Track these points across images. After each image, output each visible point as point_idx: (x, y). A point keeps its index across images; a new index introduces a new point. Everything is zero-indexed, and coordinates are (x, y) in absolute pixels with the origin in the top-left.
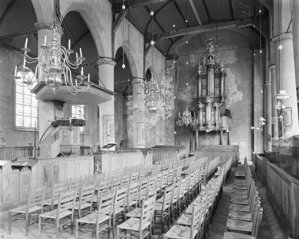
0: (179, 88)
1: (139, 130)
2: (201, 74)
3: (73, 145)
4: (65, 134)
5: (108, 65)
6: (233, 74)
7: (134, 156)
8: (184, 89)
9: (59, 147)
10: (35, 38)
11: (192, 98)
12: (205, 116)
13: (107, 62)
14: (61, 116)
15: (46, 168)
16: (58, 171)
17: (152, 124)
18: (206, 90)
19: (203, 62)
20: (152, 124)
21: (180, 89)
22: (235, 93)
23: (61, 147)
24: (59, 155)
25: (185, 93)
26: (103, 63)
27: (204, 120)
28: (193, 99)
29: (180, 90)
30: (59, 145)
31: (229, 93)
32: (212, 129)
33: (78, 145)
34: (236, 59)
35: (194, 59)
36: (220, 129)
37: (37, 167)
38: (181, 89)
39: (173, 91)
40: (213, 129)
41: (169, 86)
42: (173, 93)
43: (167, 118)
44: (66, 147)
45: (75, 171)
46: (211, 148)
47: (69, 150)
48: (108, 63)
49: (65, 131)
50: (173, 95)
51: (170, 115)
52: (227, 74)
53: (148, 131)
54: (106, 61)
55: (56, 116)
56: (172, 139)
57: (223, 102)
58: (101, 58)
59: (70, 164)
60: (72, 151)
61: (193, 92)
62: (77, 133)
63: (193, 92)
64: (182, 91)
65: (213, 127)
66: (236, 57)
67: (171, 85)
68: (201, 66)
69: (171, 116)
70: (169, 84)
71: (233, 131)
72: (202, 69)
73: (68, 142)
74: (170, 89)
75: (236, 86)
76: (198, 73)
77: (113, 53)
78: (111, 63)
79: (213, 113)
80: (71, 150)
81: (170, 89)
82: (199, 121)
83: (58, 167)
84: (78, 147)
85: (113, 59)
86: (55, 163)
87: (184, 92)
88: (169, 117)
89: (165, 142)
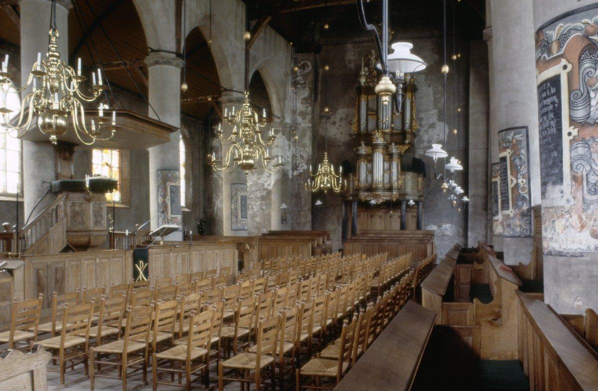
1: (235, 199)
2: (367, 85)
3: (94, 229)
4: (77, 208)
5: (167, 66)
6: (429, 86)
7: (217, 251)
8: (332, 115)
9: (65, 233)
10: (14, 13)
11: (349, 132)
12: (371, 172)
13: (165, 60)
14: (69, 171)
15: (41, 272)
16: (63, 278)
17: (266, 186)
18: (375, 117)
19: (370, 60)
20: (266, 186)
22: (432, 126)
23: (69, 233)
24: (66, 249)
25: (334, 123)
26: (157, 63)
27: (369, 179)
28: (351, 135)
30: (65, 229)
31: (421, 125)
33: (104, 231)
35: (352, 53)
37: (23, 271)
39: (309, 117)
40: (388, 198)
41: (300, 107)
42: (310, 123)
43: (295, 173)
44: (80, 234)
45: (96, 279)
46: (380, 235)
47: (85, 240)
48: (168, 63)
49: (78, 201)
50: (308, 127)
51: (303, 168)
52: (418, 87)
53: (257, 201)
54: (163, 58)
55: (59, 172)
56: (306, 218)
57: (409, 143)
58: (153, 51)
59: (85, 265)
60: (91, 241)
61: (351, 120)
62: (102, 206)
63: (351, 120)
67: (305, 106)
68: (366, 69)
69: (304, 170)
70: (301, 103)
71: (429, 203)
72: (367, 74)
73: (83, 223)
74: (303, 114)
75: (434, 112)
76: (360, 83)
77: (178, 41)
78: (175, 63)
79: (387, 165)
80: (90, 240)
81: (303, 114)
82: (359, 180)
83: (63, 271)
84: (104, 233)
85: (178, 55)
86: (58, 263)
87: (332, 120)
88: (301, 171)
89: (292, 224)
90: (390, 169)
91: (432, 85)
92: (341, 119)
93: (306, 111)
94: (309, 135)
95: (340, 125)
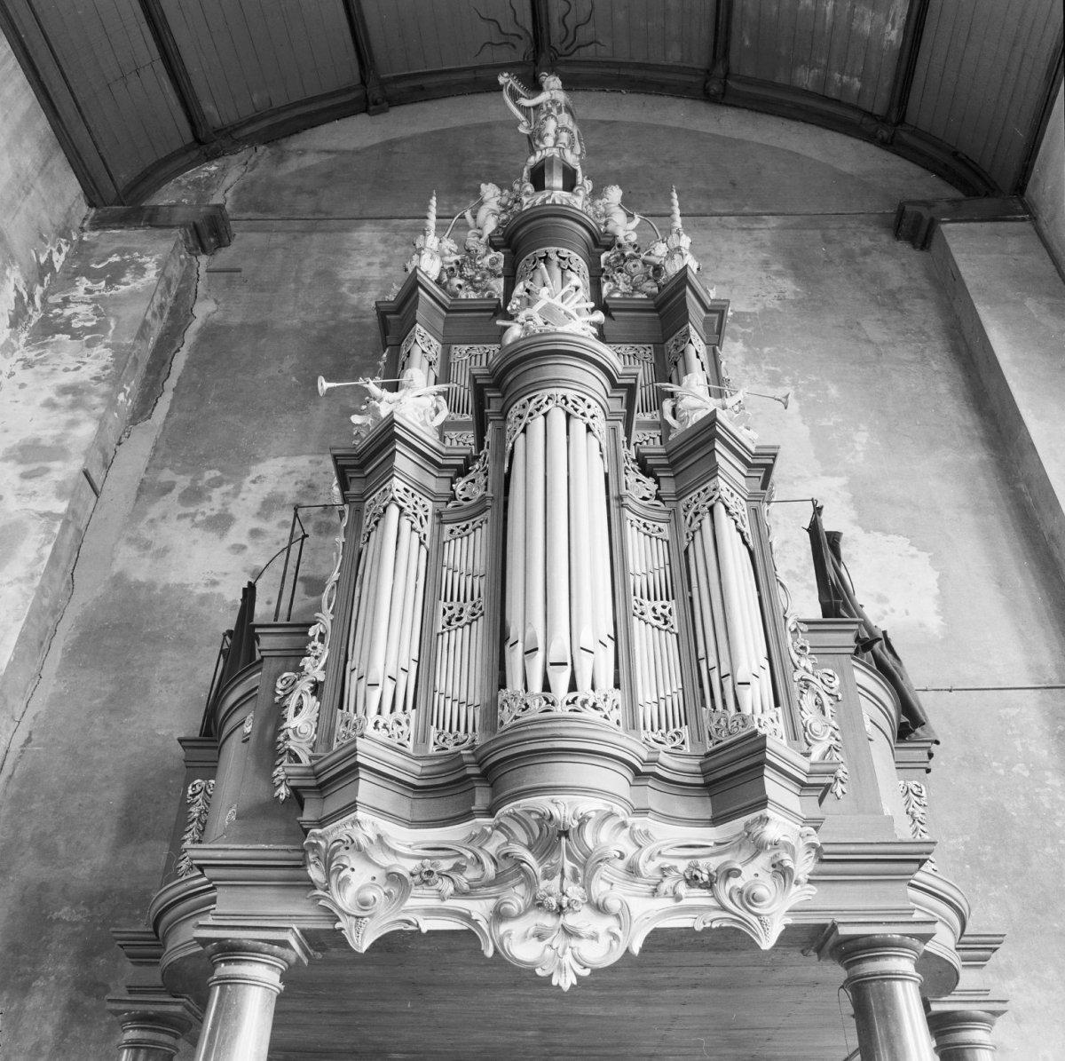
0: (153, 465)
8: (218, 482)
21: (166, 476)
25: (221, 523)
27: (460, 673)
29: (167, 489)
32: (649, 913)
34: (789, 286)
36: (853, 907)
38: (183, 482)
40: (694, 912)
64: (194, 495)
65: (676, 834)
66: (779, 274)
79: (646, 556)
90: (684, 582)
91: (787, 379)
92: (269, 506)
93: (59, 439)
94: (32, 556)
95: (255, 533)
